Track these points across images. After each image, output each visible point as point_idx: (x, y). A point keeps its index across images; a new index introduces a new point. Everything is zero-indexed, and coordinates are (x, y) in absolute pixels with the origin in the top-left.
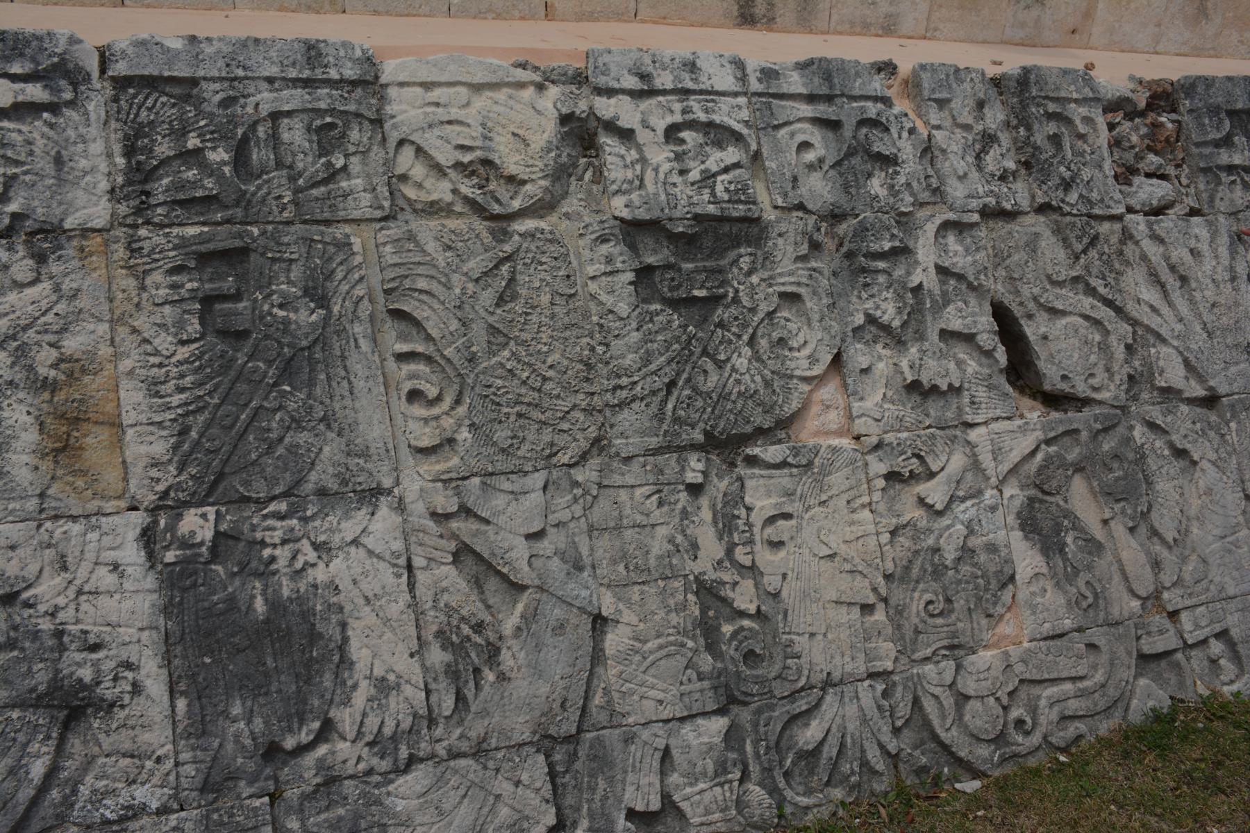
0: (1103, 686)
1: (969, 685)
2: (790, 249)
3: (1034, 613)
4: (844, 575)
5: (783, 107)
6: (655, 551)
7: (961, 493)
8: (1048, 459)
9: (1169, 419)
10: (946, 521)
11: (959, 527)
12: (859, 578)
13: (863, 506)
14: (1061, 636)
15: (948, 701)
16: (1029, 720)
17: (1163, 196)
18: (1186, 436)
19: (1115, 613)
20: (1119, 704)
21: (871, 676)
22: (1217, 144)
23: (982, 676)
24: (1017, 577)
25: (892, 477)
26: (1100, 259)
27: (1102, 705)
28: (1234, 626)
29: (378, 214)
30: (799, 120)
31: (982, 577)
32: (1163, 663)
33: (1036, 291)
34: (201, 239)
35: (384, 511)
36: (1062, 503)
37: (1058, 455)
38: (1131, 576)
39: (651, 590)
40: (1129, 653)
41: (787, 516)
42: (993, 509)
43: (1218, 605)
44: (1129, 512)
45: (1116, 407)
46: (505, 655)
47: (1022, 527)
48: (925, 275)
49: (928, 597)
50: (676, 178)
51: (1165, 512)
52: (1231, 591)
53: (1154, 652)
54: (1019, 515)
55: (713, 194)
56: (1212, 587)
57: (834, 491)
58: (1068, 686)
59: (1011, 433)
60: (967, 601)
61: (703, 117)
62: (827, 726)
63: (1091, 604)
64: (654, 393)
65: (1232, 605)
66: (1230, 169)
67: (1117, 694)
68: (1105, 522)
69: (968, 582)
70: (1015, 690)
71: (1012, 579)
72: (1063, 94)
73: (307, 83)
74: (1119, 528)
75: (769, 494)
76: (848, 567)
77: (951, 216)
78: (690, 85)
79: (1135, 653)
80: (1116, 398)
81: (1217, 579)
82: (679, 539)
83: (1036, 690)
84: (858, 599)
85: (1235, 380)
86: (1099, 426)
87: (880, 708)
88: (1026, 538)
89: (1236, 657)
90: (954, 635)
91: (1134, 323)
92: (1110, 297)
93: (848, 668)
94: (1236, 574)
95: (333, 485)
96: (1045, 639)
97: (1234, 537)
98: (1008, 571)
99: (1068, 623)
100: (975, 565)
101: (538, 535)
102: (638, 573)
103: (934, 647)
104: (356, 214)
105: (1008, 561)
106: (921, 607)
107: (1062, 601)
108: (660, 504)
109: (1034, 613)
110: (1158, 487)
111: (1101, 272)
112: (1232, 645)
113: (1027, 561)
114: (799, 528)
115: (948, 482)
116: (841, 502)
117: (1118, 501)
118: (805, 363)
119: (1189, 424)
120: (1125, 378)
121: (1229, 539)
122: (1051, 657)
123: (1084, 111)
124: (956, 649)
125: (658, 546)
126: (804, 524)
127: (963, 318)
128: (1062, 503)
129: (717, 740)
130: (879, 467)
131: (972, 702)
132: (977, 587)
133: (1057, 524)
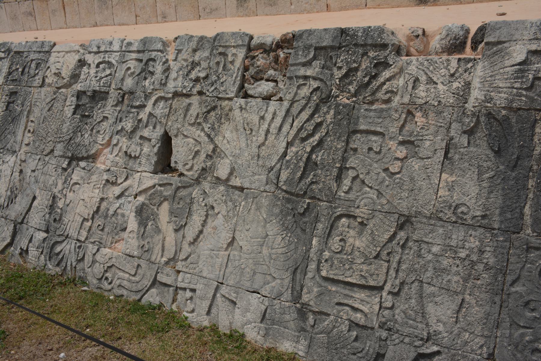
0: (137, 282)
2: (112, 102)
3: (126, 244)
5: (128, 55)
6: (50, 183)
8: (156, 192)
9: (211, 191)
17: (268, 90)
18: (216, 200)
21: (78, 240)
22: (304, 65)
25: (107, 181)
26: (215, 117)
27: (134, 289)
28: (199, 290)
29: (39, 85)
30: (131, 60)
32: (166, 289)
33: (179, 126)
34: (12, 89)
35: (14, 156)
37: (161, 191)
38: (166, 248)
39: (45, 193)
41: (79, 184)
42: (130, 202)
43: (196, 277)
45: (192, 179)
46: (17, 198)
47: (136, 212)
48: (143, 116)
50: (93, 79)
51: (191, 229)
52: (204, 275)
54: (137, 207)
55: (100, 84)
56: (197, 269)
57: (92, 181)
58: (127, 276)
59: (145, 178)
61: (107, 59)
63: (146, 251)
64: (66, 140)
65: (202, 281)
66: (306, 78)
67: (141, 288)
72: (228, 44)
73: (40, 52)
75: (78, 176)
76: (85, 205)
77: (163, 95)
78: (108, 49)
80: (192, 175)
81: (201, 266)
82: (55, 181)
83: (117, 271)
85: (254, 182)
86: (180, 185)
87: (75, 251)
91: (216, 147)
92: (209, 133)
94: (210, 268)
95: (10, 149)
96: (125, 254)
97: (217, 252)
98: (125, 225)
99: (136, 253)
100: (117, 219)
101: (34, 171)
102: (46, 188)
103: (95, 240)
104: (35, 85)
105: (126, 222)
107: (137, 244)
108: (56, 171)
109: (126, 244)
110: (194, 217)
111: (214, 122)
114: (79, 189)
115: (122, 188)
116: (92, 185)
118: (101, 139)
119: (220, 196)
120: (201, 168)
121: (215, 252)
122: (124, 262)
123: (234, 51)
124: (100, 245)
125: (51, 182)
127: (150, 132)
129: (41, 239)
130: (105, 177)
133: (148, 216)
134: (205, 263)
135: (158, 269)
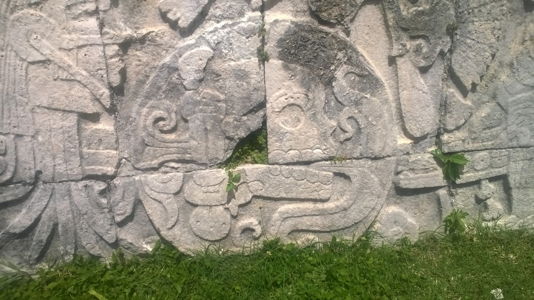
0: (345, 209)
1: (197, 195)
4: (59, 83)
7: (218, 12)
10: (190, 40)
11: (205, 48)
12: (78, 87)
13: (90, 14)
14: (307, 163)
15: (172, 205)
16: (258, 230)
19: (377, 148)
20: (362, 226)
23: (211, 189)
24: (268, 105)
31: (225, 101)
36: (342, 35)
40: (383, 185)
44: (425, 50)
49: (157, 113)
51: (471, 55)
52: (524, 141)
53: (412, 187)
58: (309, 206)
60: (204, 122)
62: (35, 216)
68: (392, 61)
69: (206, 104)
70: (249, 202)
71: (262, 105)
74: (405, 67)
79: (390, 185)
84: (74, 108)
88: (286, 68)
89: (508, 200)
90: (185, 151)
93: (61, 169)
98: (256, 97)
99: (318, 153)
103: (161, 159)
106: (150, 121)
112: (507, 189)
113: (282, 91)
117: (413, 38)
126: (9, 24)
128: (342, 35)
131: (197, 209)
132: (218, 110)
134: (522, 118)
135: (396, 168)
